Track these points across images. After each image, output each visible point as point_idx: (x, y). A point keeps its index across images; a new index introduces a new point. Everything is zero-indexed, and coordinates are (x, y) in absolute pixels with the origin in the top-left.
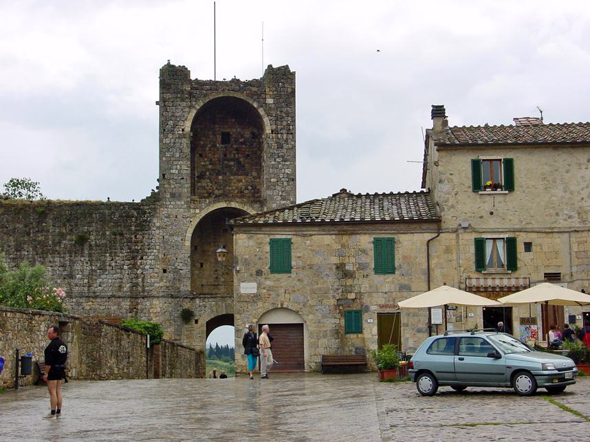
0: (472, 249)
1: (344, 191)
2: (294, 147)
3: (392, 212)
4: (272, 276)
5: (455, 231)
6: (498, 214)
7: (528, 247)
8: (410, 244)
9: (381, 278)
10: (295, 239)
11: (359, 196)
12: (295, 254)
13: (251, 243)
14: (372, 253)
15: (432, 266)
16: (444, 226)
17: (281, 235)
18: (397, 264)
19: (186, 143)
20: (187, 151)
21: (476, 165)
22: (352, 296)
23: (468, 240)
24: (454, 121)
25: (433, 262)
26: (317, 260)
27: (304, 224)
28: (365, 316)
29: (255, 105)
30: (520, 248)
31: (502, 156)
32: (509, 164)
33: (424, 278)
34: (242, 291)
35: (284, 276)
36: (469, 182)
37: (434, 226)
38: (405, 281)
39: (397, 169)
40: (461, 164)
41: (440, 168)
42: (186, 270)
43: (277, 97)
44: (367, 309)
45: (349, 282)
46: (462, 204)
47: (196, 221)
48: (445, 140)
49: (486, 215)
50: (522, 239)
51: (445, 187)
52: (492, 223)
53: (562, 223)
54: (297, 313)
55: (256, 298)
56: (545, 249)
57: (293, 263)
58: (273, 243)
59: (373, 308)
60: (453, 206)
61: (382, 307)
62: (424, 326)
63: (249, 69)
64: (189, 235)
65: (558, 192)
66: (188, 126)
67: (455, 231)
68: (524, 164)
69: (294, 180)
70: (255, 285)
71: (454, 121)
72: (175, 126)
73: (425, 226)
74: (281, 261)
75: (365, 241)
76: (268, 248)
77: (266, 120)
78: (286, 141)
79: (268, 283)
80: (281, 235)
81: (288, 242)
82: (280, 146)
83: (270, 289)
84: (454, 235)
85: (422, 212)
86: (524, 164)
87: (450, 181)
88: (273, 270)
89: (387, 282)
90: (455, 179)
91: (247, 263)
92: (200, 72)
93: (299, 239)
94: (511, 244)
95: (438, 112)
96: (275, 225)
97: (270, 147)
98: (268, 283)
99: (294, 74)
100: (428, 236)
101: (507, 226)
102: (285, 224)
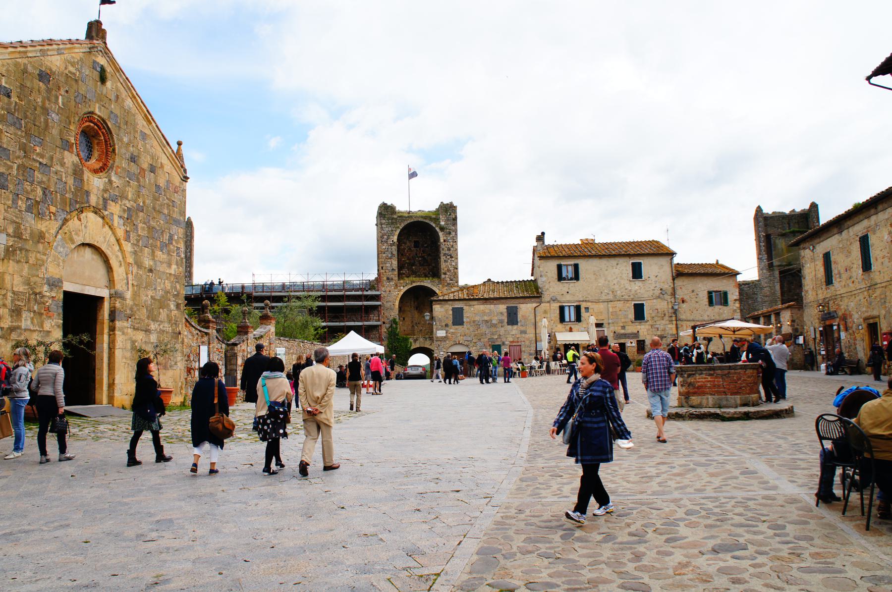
0: (558, 312)
1: (489, 280)
2: (456, 250)
3: (515, 293)
5: (549, 302)
6: (570, 293)
7: (587, 309)
8: (525, 309)
9: (510, 327)
10: (465, 308)
11: (498, 283)
14: (506, 314)
16: (543, 300)
19: (394, 248)
20: (395, 253)
21: (559, 267)
23: (556, 306)
24: (548, 241)
26: (477, 318)
27: (470, 300)
29: (434, 225)
30: (583, 310)
31: (572, 262)
32: (576, 267)
33: (533, 327)
34: (438, 335)
35: (460, 327)
36: (556, 276)
37: (537, 300)
38: (523, 329)
39: (519, 269)
40: (551, 267)
44: (504, 344)
45: (494, 330)
46: (552, 287)
48: (545, 252)
50: (583, 305)
51: (544, 279)
52: (568, 297)
53: (604, 298)
54: (467, 346)
55: (445, 339)
58: (453, 309)
59: (507, 343)
63: (431, 206)
65: (602, 282)
66: (395, 238)
67: (549, 302)
68: (583, 265)
71: (548, 241)
73: (533, 300)
74: (458, 318)
75: (502, 308)
76: (451, 312)
77: (441, 234)
82: (449, 250)
84: (548, 304)
85: (530, 290)
86: (583, 265)
87: (546, 276)
89: (514, 330)
91: (440, 321)
92: (401, 207)
94: (578, 309)
95: (540, 238)
96: (455, 300)
99: (455, 207)
100: (535, 305)
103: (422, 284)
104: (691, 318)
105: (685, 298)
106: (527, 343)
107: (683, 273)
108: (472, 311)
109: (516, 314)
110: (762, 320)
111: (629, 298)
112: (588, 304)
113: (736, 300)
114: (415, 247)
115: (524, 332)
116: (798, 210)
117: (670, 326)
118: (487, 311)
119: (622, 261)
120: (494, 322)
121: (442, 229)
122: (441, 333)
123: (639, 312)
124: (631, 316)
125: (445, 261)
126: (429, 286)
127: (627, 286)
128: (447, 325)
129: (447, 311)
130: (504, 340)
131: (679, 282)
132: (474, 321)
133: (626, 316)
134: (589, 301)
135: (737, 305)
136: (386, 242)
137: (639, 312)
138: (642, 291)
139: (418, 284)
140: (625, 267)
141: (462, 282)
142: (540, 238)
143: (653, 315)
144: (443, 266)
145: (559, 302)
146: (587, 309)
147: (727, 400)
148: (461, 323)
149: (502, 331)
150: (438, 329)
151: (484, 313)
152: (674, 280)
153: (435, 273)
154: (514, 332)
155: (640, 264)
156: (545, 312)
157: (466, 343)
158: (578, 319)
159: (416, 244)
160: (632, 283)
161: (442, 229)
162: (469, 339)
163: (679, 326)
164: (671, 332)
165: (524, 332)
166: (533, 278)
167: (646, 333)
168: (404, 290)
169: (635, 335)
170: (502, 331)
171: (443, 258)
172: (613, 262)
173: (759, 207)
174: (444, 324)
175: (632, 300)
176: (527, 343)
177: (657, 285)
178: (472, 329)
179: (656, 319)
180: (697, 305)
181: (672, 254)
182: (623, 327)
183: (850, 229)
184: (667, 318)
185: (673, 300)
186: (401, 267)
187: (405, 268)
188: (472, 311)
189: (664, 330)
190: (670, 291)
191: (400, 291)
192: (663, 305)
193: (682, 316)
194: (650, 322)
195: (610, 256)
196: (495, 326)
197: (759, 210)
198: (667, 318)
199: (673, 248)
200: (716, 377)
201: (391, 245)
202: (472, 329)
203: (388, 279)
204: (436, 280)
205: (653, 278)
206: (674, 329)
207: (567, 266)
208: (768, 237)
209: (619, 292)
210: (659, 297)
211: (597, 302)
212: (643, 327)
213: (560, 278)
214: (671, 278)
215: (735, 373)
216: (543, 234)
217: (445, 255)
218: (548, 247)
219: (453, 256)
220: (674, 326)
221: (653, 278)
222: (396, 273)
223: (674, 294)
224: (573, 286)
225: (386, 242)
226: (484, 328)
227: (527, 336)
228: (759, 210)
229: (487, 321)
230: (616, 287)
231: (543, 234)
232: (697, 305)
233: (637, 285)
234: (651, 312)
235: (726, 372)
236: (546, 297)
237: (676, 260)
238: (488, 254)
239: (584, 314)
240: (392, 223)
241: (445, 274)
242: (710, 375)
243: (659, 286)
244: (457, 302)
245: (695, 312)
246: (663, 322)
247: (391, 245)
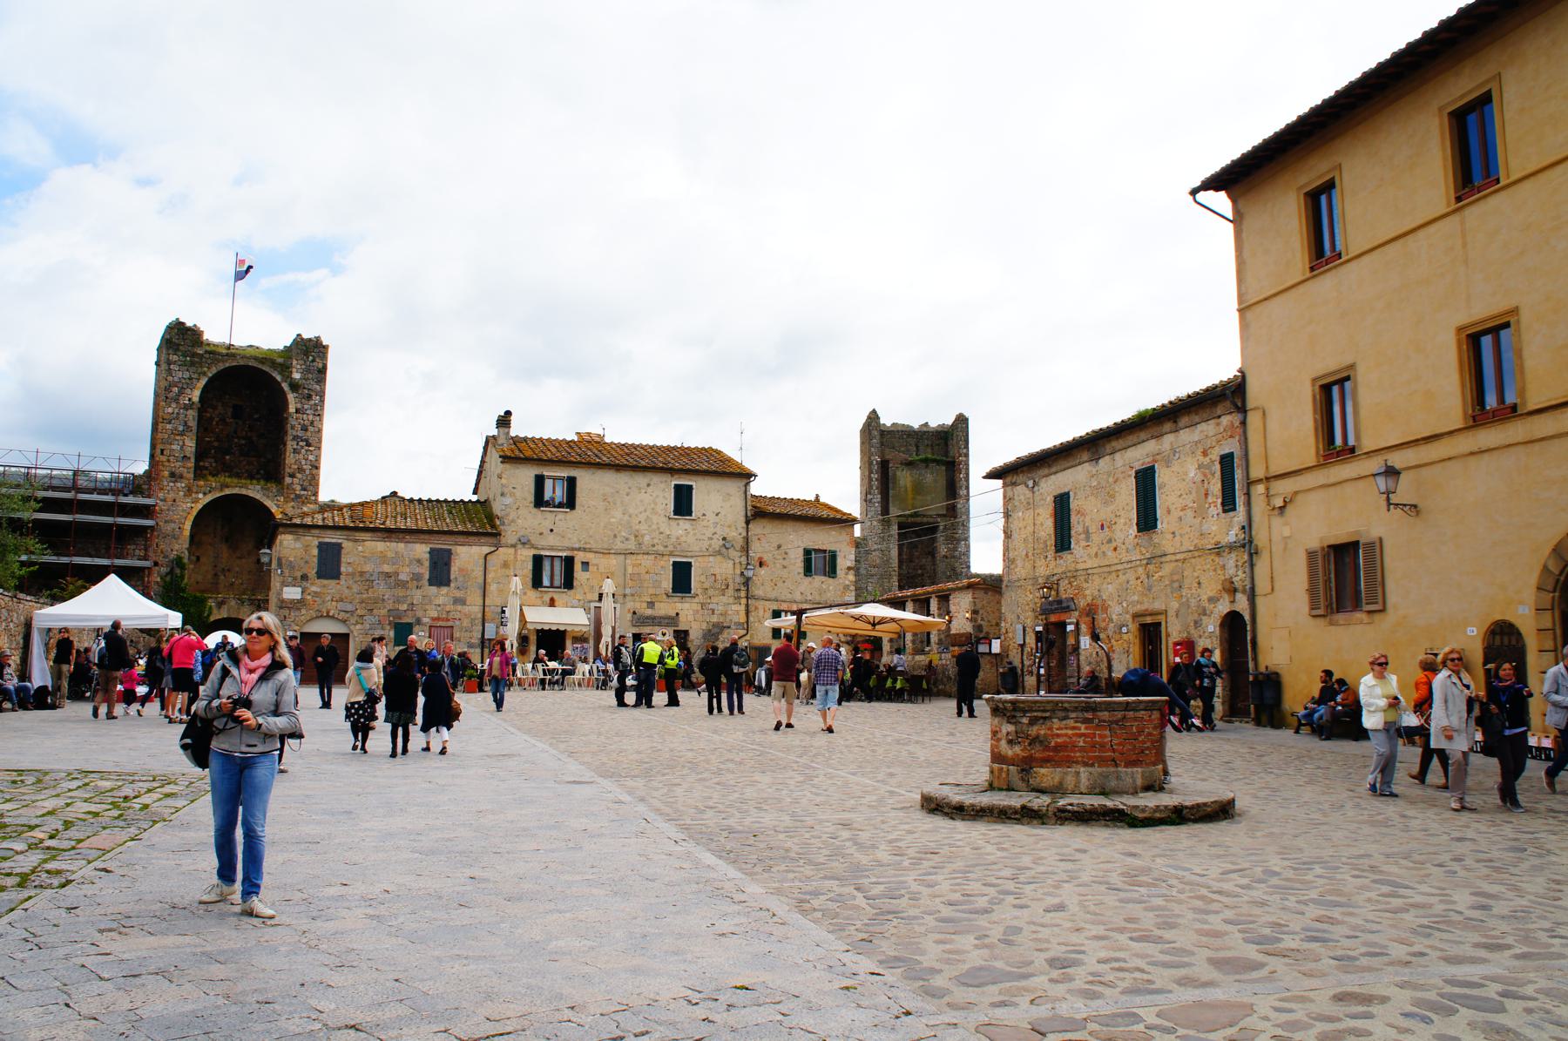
0: (530, 566)
1: (394, 494)
2: (320, 431)
3: (448, 523)
4: (318, 581)
5: (513, 546)
6: (557, 532)
7: (585, 564)
8: (467, 556)
9: (434, 589)
10: (346, 544)
11: (411, 500)
12: (345, 559)
13: (298, 545)
14: (427, 564)
16: (503, 541)
17: (331, 538)
19: (192, 414)
20: (193, 424)
21: (540, 481)
22: (405, 607)
23: (527, 554)
24: (517, 429)
25: (490, 576)
26: (368, 568)
29: (279, 378)
30: (578, 566)
31: (565, 473)
32: (572, 482)
35: (332, 583)
36: (531, 498)
38: (459, 594)
41: (504, 481)
43: (307, 371)
44: (419, 622)
45: (400, 592)
46: (521, 517)
47: (200, 506)
48: (509, 450)
49: (546, 532)
50: (579, 557)
51: (508, 500)
52: (551, 540)
53: (619, 546)
54: (344, 621)
56: (602, 569)
57: (343, 569)
58: (321, 546)
59: (425, 620)
61: (434, 619)
64: (188, 526)
65: (617, 514)
66: (196, 395)
67: (513, 546)
68: (587, 482)
69: (317, 468)
71: (517, 429)
72: (181, 393)
73: (483, 540)
74: (329, 562)
75: (421, 550)
76: (315, 552)
77: (291, 397)
78: (312, 423)
80: (331, 538)
81: (339, 547)
82: (305, 429)
84: (512, 550)
85: (479, 519)
86: (587, 482)
87: (513, 495)
89: (441, 596)
90: (518, 494)
91: (292, 567)
92: (214, 334)
93: (350, 544)
94: (569, 562)
95: (504, 421)
96: (325, 527)
97: (293, 427)
98: (314, 589)
99: (326, 347)
100: (486, 550)
101: (567, 544)
102: (336, 528)
103: (244, 492)
104: (772, 595)
105: (765, 558)
106: (466, 623)
107: (763, 512)
108: (359, 553)
109: (448, 564)
110: (909, 605)
111: (666, 551)
112: (589, 557)
113: (849, 568)
114: (235, 416)
116: (933, 424)
117: (735, 607)
118: (390, 554)
120: (403, 577)
121: (295, 387)
123: (682, 577)
124: (667, 584)
126: (258, 497)
127: (664, 527)
128: (304, 577)
129: (307, 548)
130: (419, 614)
131: (757, 528)
132: (362, 573)
133: (657, 584)
134: (590, 551)
135: (851, 577)
136: (176, 400)
137: (682, 577)
138: (690, 539)
139: (236, 491)
140: (662, 492)
141: (324, 497)
142: (504, 421)
143: (707, 585)
144: (290, 459)
145: (533, 547)
146: (585, 564)
147: (1118, 778)
148: (336, 575)
149: (417, 596)
150: (284, 584)
151: (383, 558)
152: (747, 523)
153: (272, 472)
154: (441, 600)
155: (690, 488)
156: (505, 565)
157: (342, 616)
158: (568, 583)
159: (238, 412)
160: (673, 523)
161: (295, 387)
162: (349, 607)
163: (752, 608)
164: (735, 619)
165: (463, 602)
166: (475, 498)
167: (691, 618)
168: (204, 500)
169: (672, 620)
170: (417, 596)
171: (291, 445)
172: (641, 479)
173: (874, 412)
174: (299, 574)
175: (671, 554)
176: (466, 623)
177: (718, 530)
178: (355, 588)
179: (711, 592)
180: (784, 573)
181: (747, 476)
182: (651, 604)
183: (1117, 456)
184: (730, 592)
185: (744, 560)
186: (201, 454)
187: (209, 459)
188: (359, 553)
189: (724, 614)
190: (740, 542)
191: (196, 501)
192: (726, 569)
193: (757, 591)
194: (701, 598)
195: (636, 469)
196: (403, 585)
197: (873, 417)
198: (730, 592)
199: (749, 465)
200: (1098, 727)
201: (186, 408)
202: (355, 588)
203: (172, 475)
204: (274, 487)
205: (711, 517)
206: (743, 613)
207: (555, 478)
208: (884, 465)
209: (647, 538)
210: (719, 553)
211: (606, 553)
212: (686, 606)
213: (540, 501)
214: (743, 519)
215: (1135, 719)
216: (508, 413)
217: (295, 438)
218: (516, 441)
219: (311, 441)
220: (743, 607)
221: (711, 517)
222: (191, 464)
223: (746, 549)
224: (563, 519)
225: (176, 400)
226: (381, 588)
227: (466, 609)
228: (873, 417)
229: (388, 575)
230: (643, 528)
231: (508, 413)
232: (784, 573)
233: (681, 527)
234: (703, 578)
235: (1119, 715)
236: (509, 536)
237: (756, 488)
238: (383, 444)
239: (579, 573)
240: (192, 364)
241: (292, 476)
242: (1085, 721)
243: (721, 532)
245: (780, 584)
246: (724, 599)
247: (186, 408)
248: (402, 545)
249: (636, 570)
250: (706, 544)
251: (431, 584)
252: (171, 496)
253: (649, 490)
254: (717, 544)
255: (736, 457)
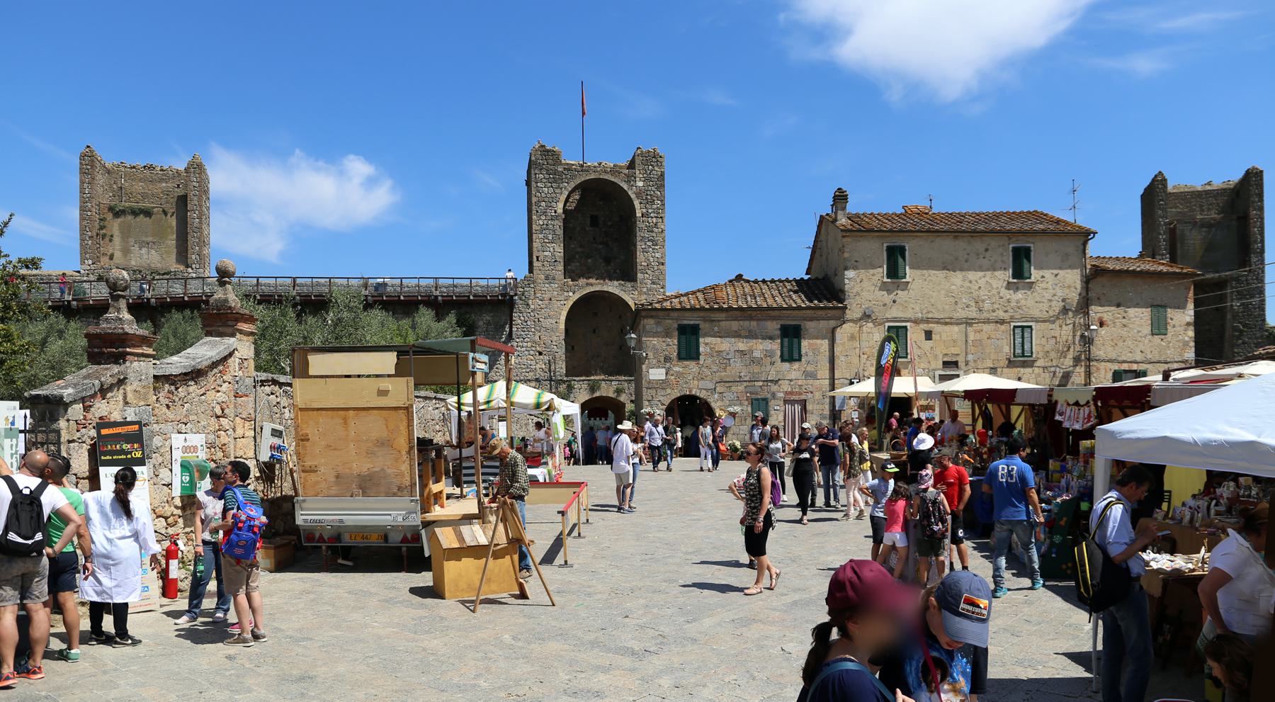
1: (739, 277)
9: (787, 365)
15: (836, 353)
18: (803, 351)
19: (558, 224)
20: (560, 232)
28: (772, 403)
29: (625, 187)
35: (692, 364)
42: (561, 352)
44: (774, 395)
45: (756, 369)
47: (570, 303)
53: (961, 314)
55: (663, 384)
60: (858, 294)
61: (786, 393)
62: (827, 412)
70: (663, 371)
77: (636, 203)
79: (677, 369)
83: (679, 375)
88: (680, 358)
95: (840, 198)
97: (641, 229)
98: (677, 369)
102: (693, 309)
104: (1114, 356)
111: (1006, 316)
113: (1188, 324)
114: (592, 225)
115: (812, 375)
119: (993, 242)
120: (757, 354)
122: (657, 374)
125: (644, 251)
126: (616, 291)
142: (840, 198)
143: (1048, 348)
144: (641, 258)
153: (627, 273)
154: (793, 375)
163: (1093, 369)
165: (812, 375)
166: (806, 277)
176: (818, 395)
179: (1053, 355)
180: (1124, 332)
181: (1085, 235)
186: (568, 260)
193: (1098, 351)
195: (974, 233)
203: (547, 278)
204: (629, 285)
222: (561, 267)
230: (983, 293)
232: (1124, 332)
243: (1060, 293)
244: (687, 314)
245: (1120, 344)
248: (754, 323)
249: (978, 336)
250: (1045, 307)
251: (783, 360)
252: (547, 296)
253: (988, 255)
254: (1057, 306)
255: (1067, 217)
